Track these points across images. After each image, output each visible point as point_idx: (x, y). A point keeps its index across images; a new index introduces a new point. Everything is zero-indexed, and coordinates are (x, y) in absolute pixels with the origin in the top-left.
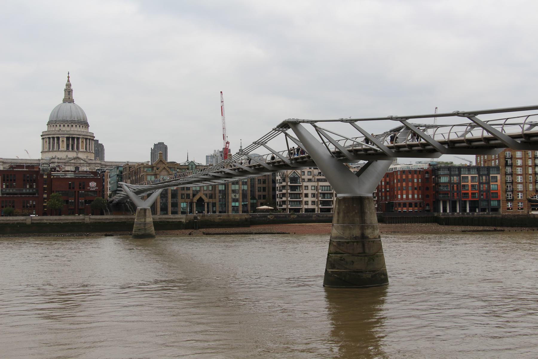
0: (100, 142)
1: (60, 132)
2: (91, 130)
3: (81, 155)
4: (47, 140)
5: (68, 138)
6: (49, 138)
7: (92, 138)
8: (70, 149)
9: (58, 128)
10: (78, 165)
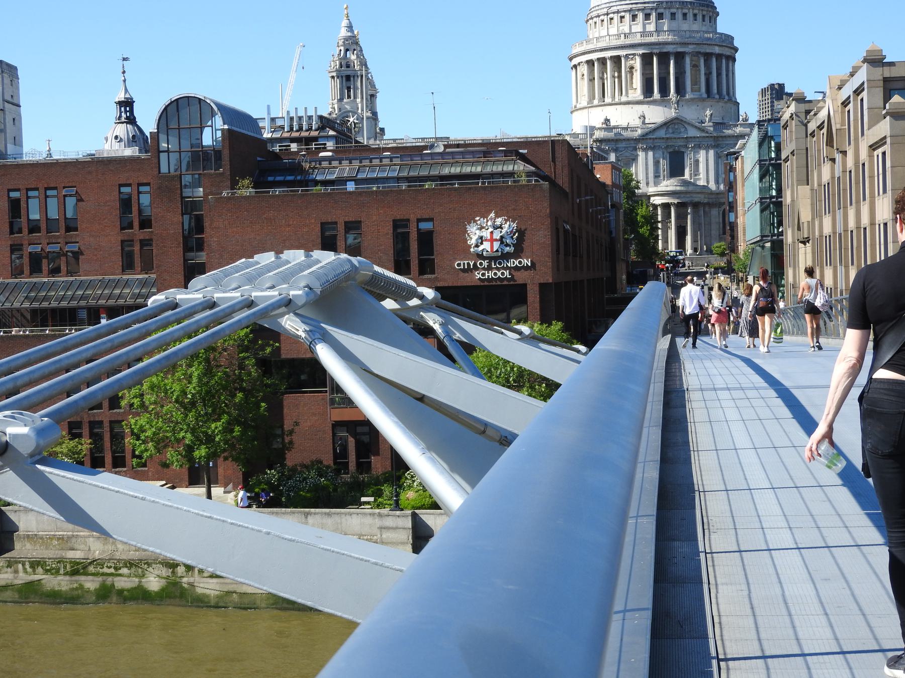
0: (788, 89)
1: (622, 41)
2: (723, 26)
3: (690, 114)
4: (584, 69)
5: (647, 60)
6: (590, 63)
7: (727, 52)
8: (656, 95)
9: (613, 31)
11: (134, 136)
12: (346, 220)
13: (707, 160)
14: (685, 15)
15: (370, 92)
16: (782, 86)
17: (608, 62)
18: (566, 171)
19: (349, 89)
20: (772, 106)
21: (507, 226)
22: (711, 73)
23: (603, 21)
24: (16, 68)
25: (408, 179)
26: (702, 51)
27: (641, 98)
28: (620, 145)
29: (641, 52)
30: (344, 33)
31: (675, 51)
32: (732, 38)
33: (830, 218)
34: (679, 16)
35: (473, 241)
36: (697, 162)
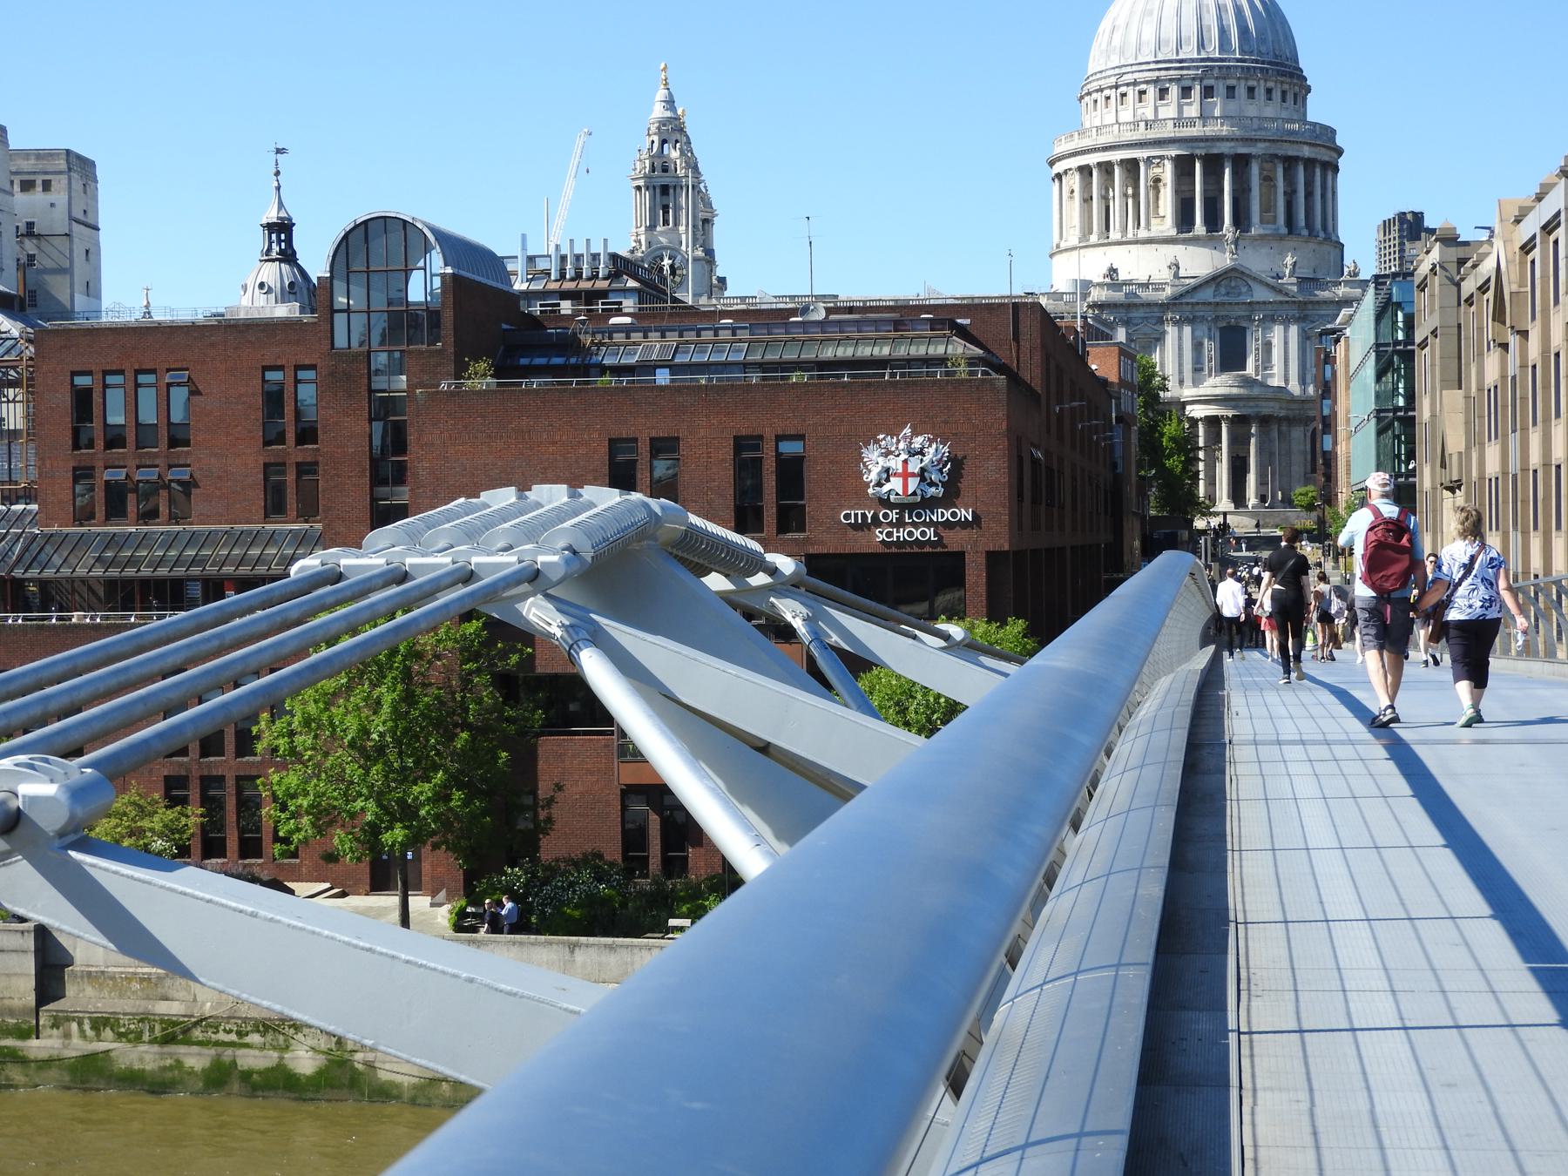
1: (1141, 134)
2: (1318, 110)
3: (1257, 262)
4: (1074, 181)
5: (1183, 167)
6: (1085, 171)
7: (1324, 155)
8: (1199, 228)
9: (1126, 115)
11: (292, 284)
12: (654, 434)
13: (1286, 343)
14: (1251, 90)
15: (701, 215)
16: (1418, 217)
17: (1117, 170)
18: (1037, 357)
19: (666, 209)
20: (1402, 251)
21: (932, 450)
22: (1294, 192)
23: (1108, 98)
24: (93, 164)
25: (762, 366)
26: (1280, 152)
27: (1173, 232)
28: (1135, 314)
29: (1174, 153)
30: (659, 111)
31: (1232, 152)
32: (1334, 132)
33: (1498, 447)
34: (1241, 91)
35: (873, 477)
36: (1268, 346)
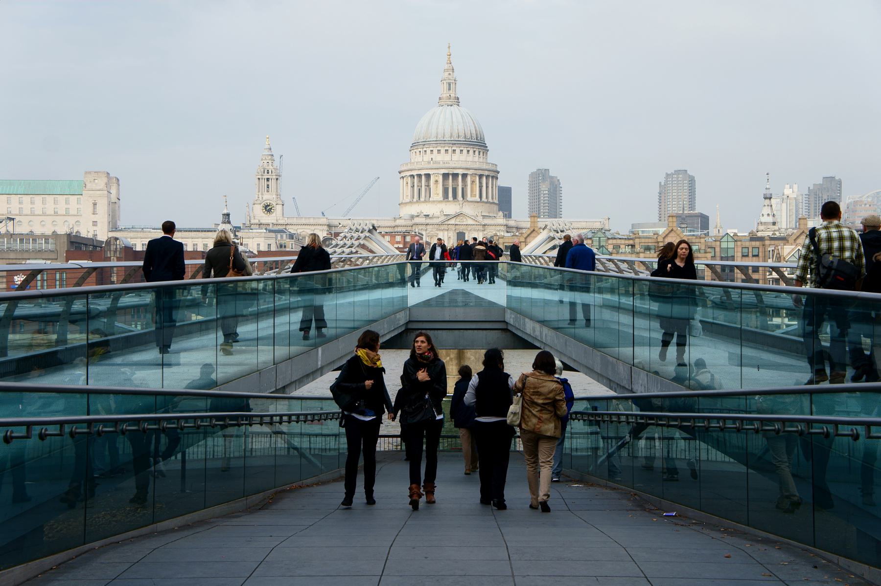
0: (551, 174)
1: (432, 165)
5: (445, 176)
6: (412, 176)
7: (492, 174)
9: (427, 157)
10: (461, 229)
16: (547, 170)
17: (423, 177)
28: (428, 227)
